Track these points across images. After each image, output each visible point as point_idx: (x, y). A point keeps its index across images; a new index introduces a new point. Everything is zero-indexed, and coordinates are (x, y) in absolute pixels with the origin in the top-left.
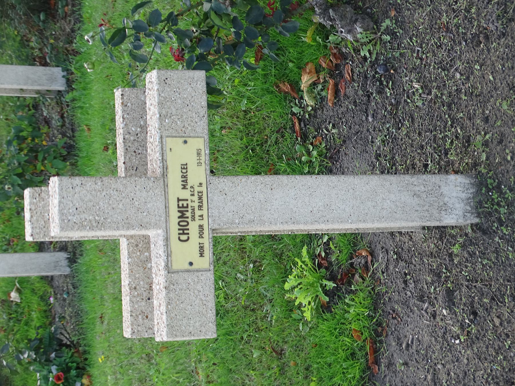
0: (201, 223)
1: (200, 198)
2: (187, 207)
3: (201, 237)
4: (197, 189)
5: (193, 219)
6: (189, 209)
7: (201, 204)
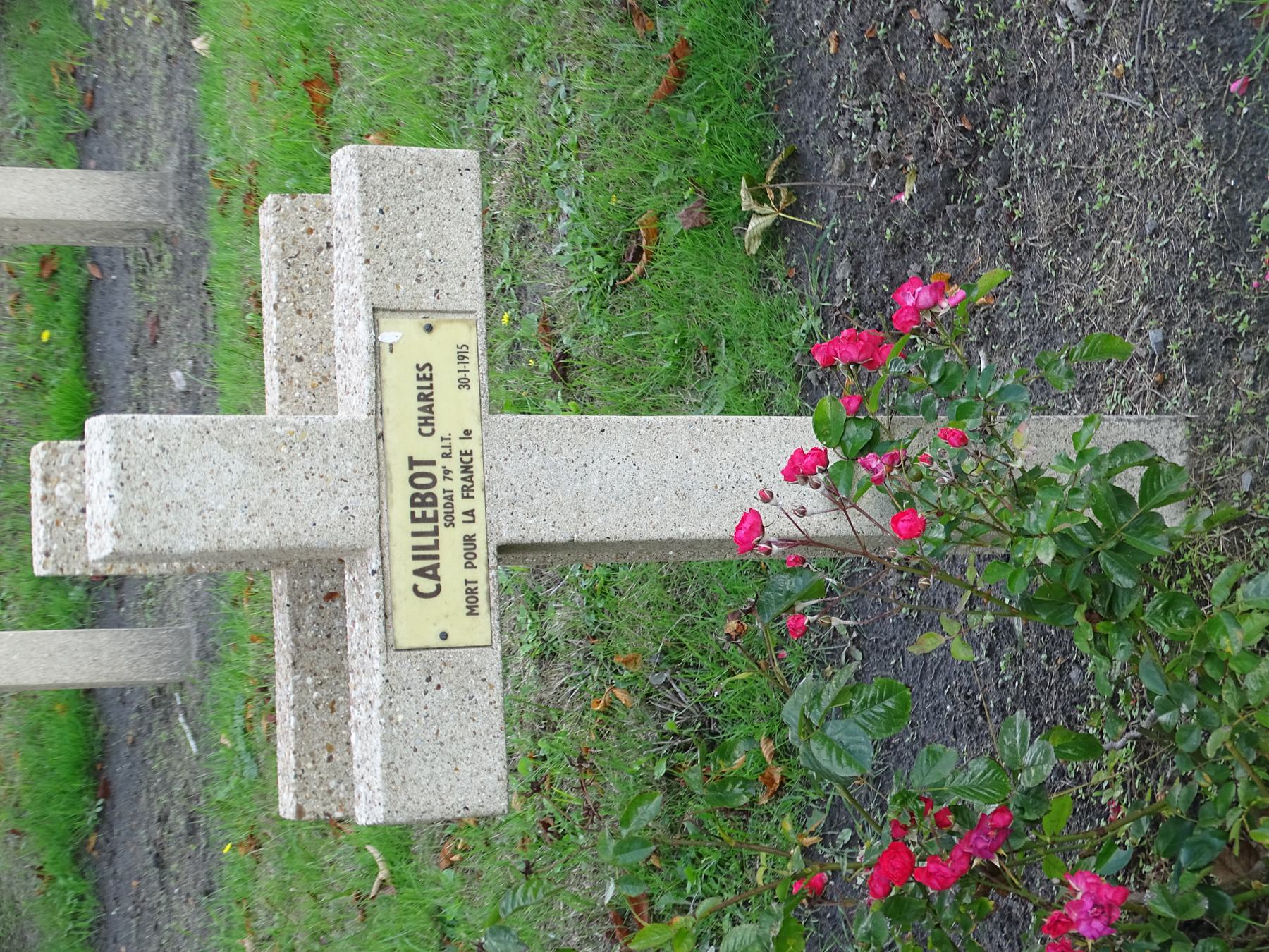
0: (470, 529)
1: (466, 468)
3: (469, 565)
4: (458, 446)
5: (450, 523)
7: (469, 484)
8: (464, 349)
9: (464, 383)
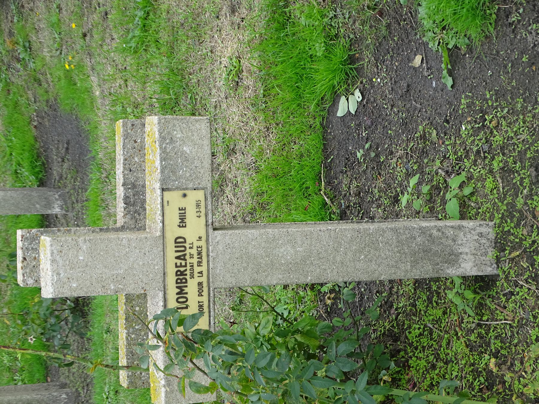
1: (199, 253)
2: (186, 266)
3: (200, 295)
5: (192, 277)
6: (188, 268)
7: (200, 260)
8: (199, 202)
9: (199, 217)
